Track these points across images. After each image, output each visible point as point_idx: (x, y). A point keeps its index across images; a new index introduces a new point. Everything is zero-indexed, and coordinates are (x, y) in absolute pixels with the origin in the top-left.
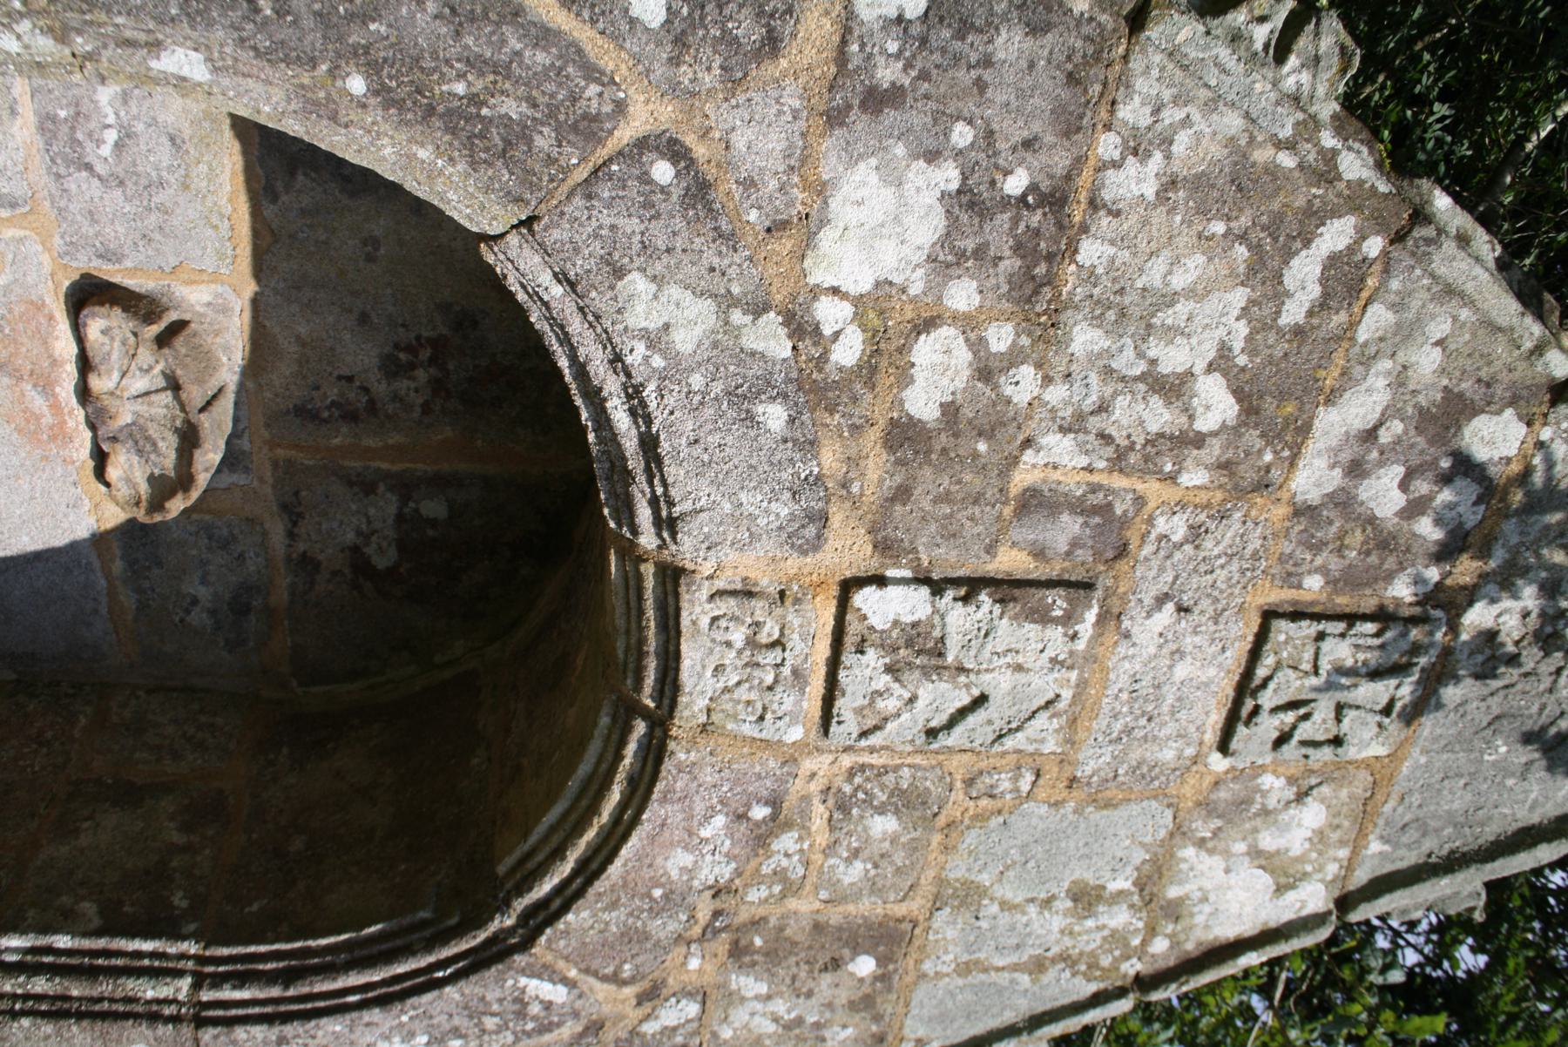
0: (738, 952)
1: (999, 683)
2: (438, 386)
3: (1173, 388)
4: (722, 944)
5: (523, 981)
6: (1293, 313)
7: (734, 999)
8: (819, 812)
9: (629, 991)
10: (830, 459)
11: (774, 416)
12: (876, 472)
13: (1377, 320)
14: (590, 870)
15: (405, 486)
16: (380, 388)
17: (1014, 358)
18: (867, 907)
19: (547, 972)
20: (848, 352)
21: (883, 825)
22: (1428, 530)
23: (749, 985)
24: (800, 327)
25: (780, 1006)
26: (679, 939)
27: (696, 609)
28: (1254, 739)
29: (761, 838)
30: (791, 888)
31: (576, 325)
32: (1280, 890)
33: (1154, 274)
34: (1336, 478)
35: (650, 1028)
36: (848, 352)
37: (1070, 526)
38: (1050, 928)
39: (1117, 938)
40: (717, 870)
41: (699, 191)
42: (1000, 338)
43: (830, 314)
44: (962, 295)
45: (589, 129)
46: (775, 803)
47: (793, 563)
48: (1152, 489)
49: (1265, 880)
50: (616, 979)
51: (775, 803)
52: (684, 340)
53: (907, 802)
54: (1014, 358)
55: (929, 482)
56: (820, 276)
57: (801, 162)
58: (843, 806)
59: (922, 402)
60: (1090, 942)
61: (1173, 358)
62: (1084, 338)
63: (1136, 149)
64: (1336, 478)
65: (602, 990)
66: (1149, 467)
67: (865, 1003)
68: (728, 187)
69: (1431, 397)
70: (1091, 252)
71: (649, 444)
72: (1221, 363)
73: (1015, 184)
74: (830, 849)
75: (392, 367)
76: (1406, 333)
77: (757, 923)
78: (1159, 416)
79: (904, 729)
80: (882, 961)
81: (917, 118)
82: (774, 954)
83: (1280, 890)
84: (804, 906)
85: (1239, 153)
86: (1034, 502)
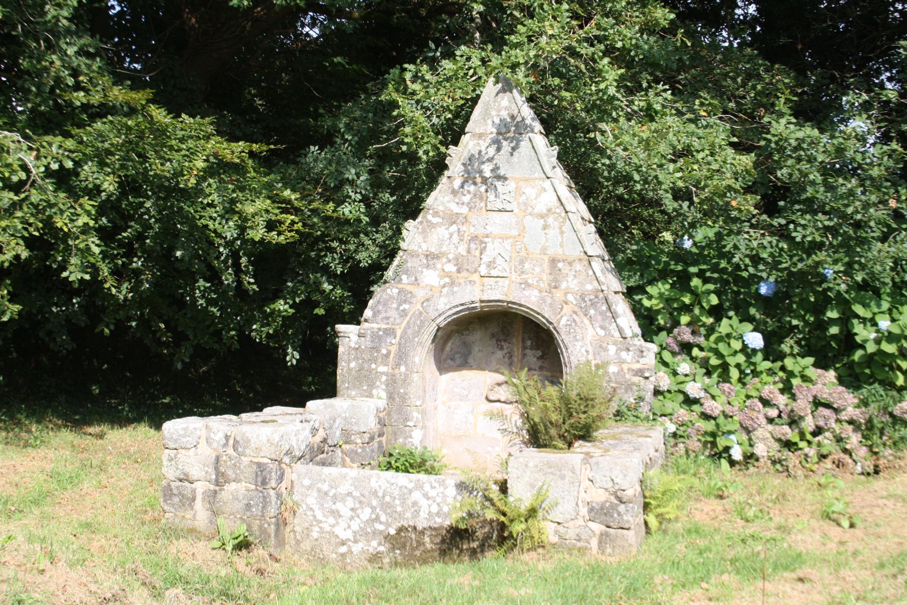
0: (556, 287)
1: (497, 252)
2: (505, 341)
3: (451, 235)
4: (554, 291)
5: (561, 324)
6: (440, 220)
7: (568, 288)
8: (524, 276)
9: (565, 306)
10: (462, 281)
11: (455, 289)
12: (464, 274)
13: (441, 208)
14: (538, 314)
15: (524, 348)
16: (506, 351)
17: (447, 258)
18: (546, 266)
19: (559, 321)
20: (447, 280)
21: (527, 266)
22: (472, 188)
23: (564, 285)
24: (444, 286)
25: (570, 279)
26: (552, 298)
27: (485, 298)
28: (513, 206)
29: (528, 285)
30: (541, 279)
31: (447, 314)
32: (545, 190)
33: (435, 241)
34: (465, 206)
35: (575, 302)
36: (447, 280)
37: (473, 246)
38: (553, 232)
39: (555, 219)
40: (536, 292)
41: (427, 300)
42: (444, 260)
43: (442, 283)
44: (439, 266)
45: (421, 313)
46: (521, 284)
47: (477, 284)
48: (466, 235)
49: (543, 195)
50: (562, 309)
51: (521, 284)
52: (446, 301)
53: (522, 262)
54: (447, 258)
55: (466, 266)
56: (437, 284)
57: (423, 288)
58: (523, 272)
59: (454, 269)
60: (557, 224)
61: (447, 236)
62: (444, 249)
63: (420, 247)
64: (465, 206)
65: (564, 311)
66: (463, 236)
67: (570, 264)
68: (427, 297)
69: (452, 196)
70: (433, 250)
71: (462, 305)
72: (447, 229)
73: (425, 261)
74: (533, 274)
75: (502, 349)
76: (442, 203)
77: (549, 285)
78: (455, 236)
79: (505, 265)
80: (559, 261)
81: (418, 274)
82: (556, 280)
83: (545, 190)
84: (545, 277)
85: (420, 233)
86: (469, 252)
